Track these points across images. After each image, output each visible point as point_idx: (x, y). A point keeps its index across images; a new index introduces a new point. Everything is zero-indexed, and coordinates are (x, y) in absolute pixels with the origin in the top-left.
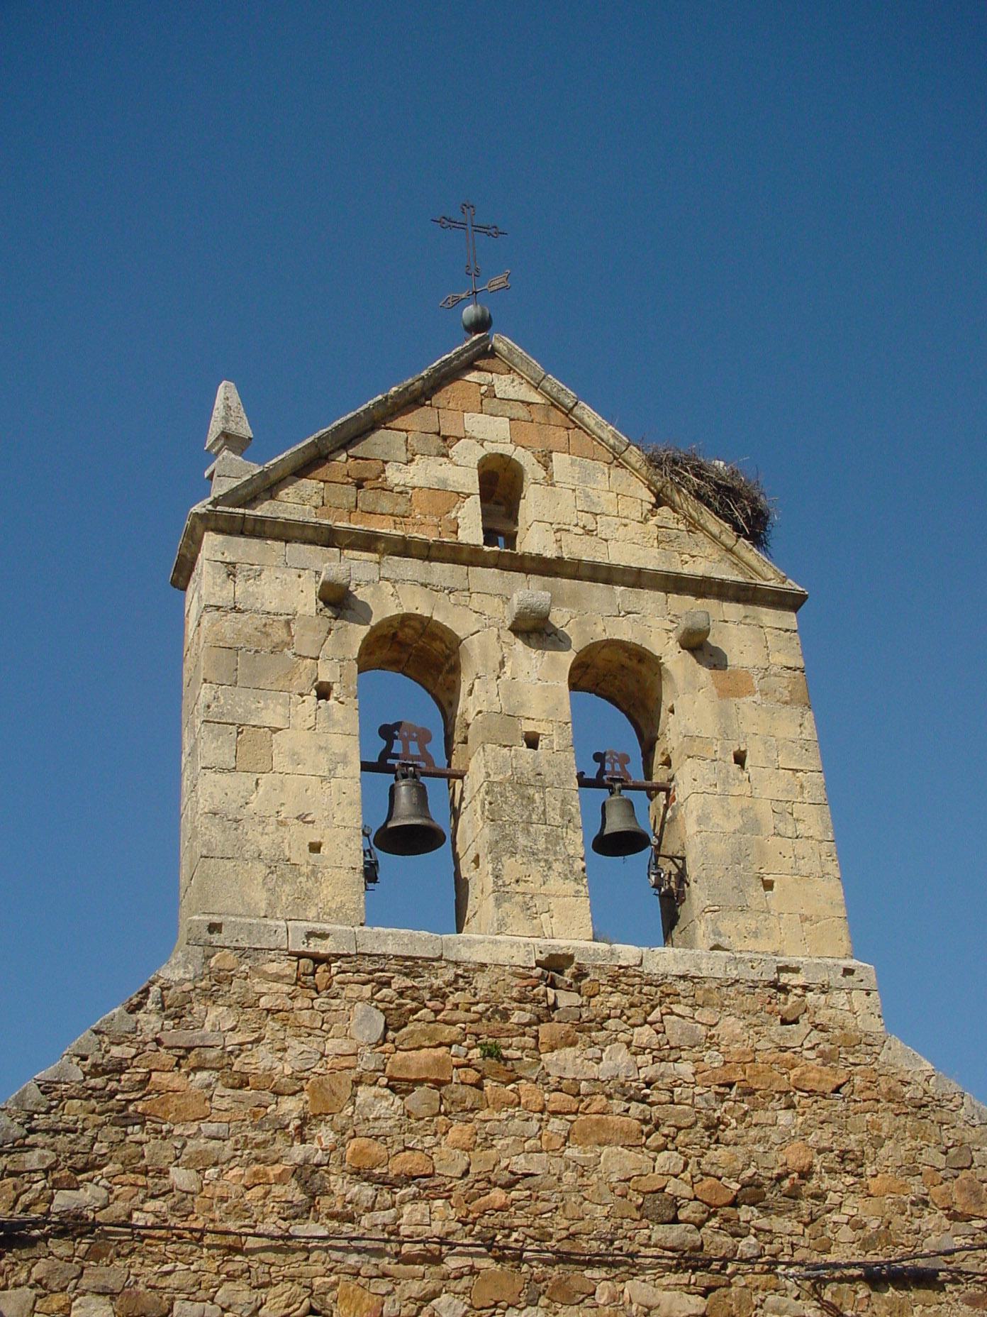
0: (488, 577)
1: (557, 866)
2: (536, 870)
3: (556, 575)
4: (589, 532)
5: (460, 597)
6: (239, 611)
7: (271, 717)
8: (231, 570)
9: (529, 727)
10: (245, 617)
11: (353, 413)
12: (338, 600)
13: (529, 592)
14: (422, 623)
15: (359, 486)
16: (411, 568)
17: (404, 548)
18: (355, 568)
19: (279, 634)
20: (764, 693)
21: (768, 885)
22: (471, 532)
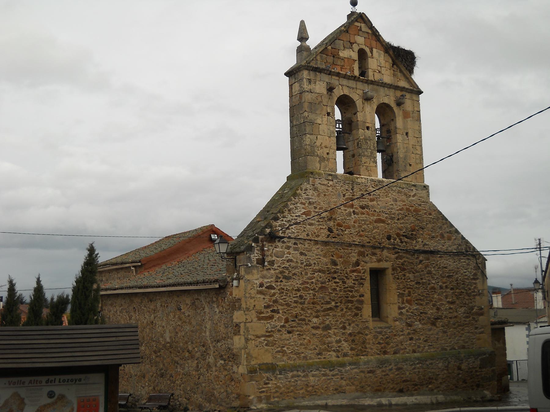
0: (360, 85)
1: (372, 160)
2: (368, 160)
3: (374, 84)
4: (379, 72)
5: (355, 90)
6: (311, 92)
7: (319, 121)
8: (310, 81)
9: (368, 125)
10: (313, 94)
11: (462, 409)
12: (330, 90)
13: (367, 88)
14: (414, 146)
15: (334, 57)
16: (345, 82)
17: (345, 77)
18: (335, 81)
19: (320, 99)
20: (413, 118)
21: (410, 165)
22: (357, 73)
